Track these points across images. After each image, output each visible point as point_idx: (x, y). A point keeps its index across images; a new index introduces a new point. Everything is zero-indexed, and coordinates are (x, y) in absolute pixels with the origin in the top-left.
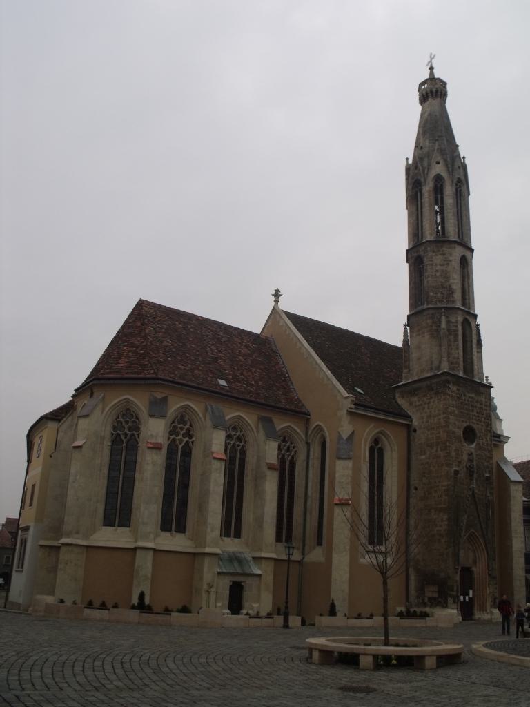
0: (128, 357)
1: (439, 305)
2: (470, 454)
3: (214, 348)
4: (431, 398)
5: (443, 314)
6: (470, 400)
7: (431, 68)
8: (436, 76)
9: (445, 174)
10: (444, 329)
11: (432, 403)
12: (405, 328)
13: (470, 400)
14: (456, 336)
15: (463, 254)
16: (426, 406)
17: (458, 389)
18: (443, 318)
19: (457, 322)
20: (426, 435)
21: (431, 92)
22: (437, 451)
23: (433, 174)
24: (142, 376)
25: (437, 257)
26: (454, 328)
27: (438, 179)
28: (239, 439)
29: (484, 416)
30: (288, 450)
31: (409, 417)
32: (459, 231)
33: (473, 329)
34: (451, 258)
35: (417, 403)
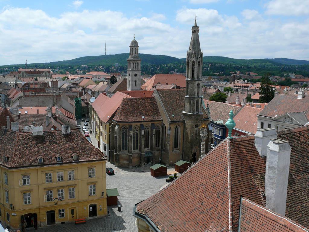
0: (123, 115)
2: (196, 130)
3: (141, 107)
7: (196, 20)
14: (195, 104)
18: (192, 100)
21: (194, 31)
23: (192, 61)
24: (127, 121)
27: (193, 62)
28: (147, 129)
30: (158, 128)
34: (195, 85)
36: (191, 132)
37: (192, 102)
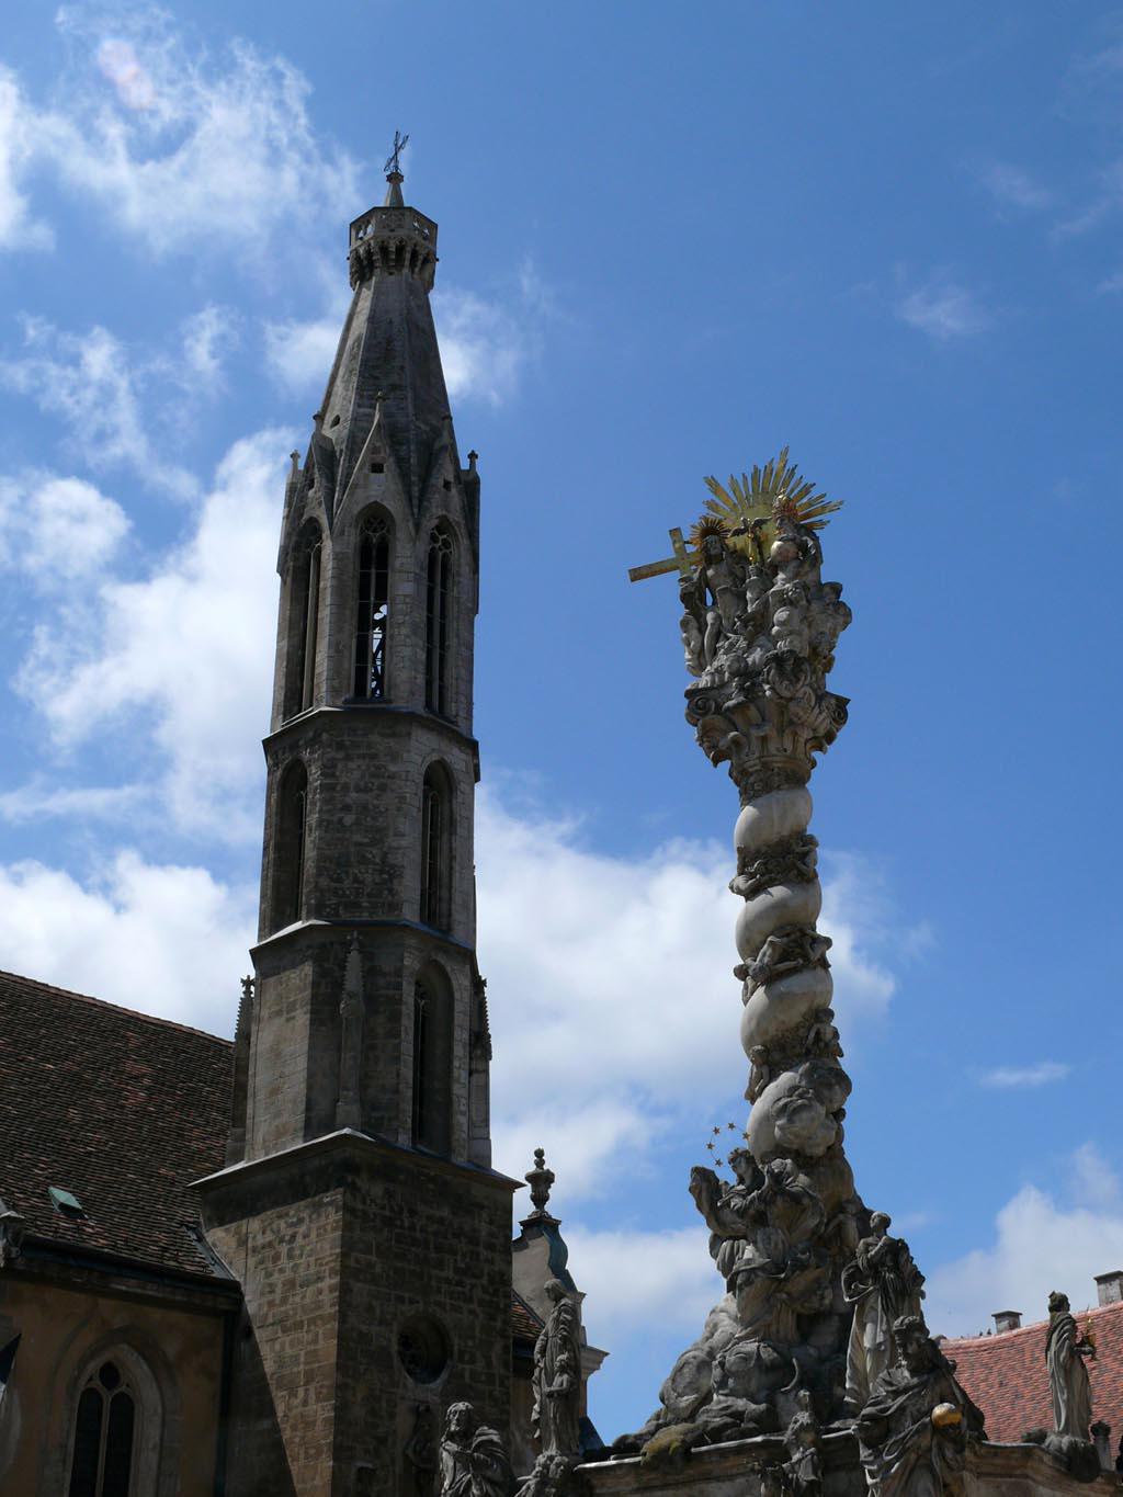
1: (345, 916)
4: (301, 1221)
5: (355, 945)
6: (433, 1228)
7: (395, 178)
8: (406, 204)
9: (395, 506)
10: (351, 995)
11: (299, 1240)
12: (248, 992)
13: (433, 1228)
14: (395, 1017)
15: (435, 757)
16: (284, 1249)
17: (389, 1194)
18: (354, 957)
19: (398, 973)
20: (277, 1347)
21: (384, 249)
22: (305, 1403)
23: (352, 503)
25: (352, 765)
26: (391, 992)
29: (485, 1281)
31: (233, 1289)
32: (429, 683)
33: (457, 995)
34: (393, 768)
35: (260, 1240)
36: (341, 1411)
37: (353, 979)
